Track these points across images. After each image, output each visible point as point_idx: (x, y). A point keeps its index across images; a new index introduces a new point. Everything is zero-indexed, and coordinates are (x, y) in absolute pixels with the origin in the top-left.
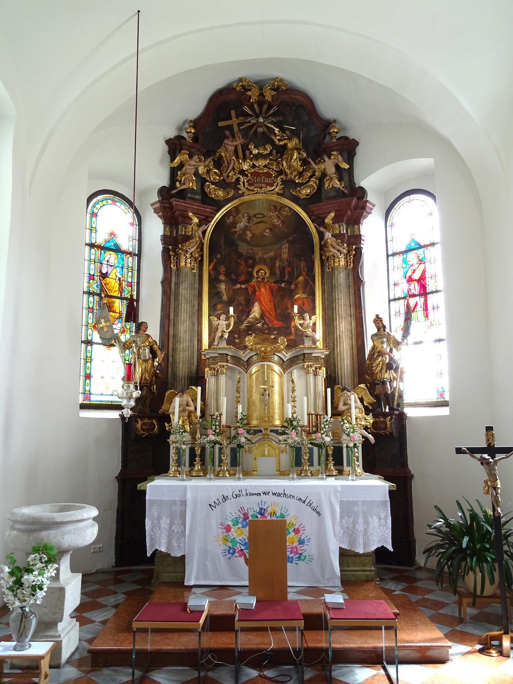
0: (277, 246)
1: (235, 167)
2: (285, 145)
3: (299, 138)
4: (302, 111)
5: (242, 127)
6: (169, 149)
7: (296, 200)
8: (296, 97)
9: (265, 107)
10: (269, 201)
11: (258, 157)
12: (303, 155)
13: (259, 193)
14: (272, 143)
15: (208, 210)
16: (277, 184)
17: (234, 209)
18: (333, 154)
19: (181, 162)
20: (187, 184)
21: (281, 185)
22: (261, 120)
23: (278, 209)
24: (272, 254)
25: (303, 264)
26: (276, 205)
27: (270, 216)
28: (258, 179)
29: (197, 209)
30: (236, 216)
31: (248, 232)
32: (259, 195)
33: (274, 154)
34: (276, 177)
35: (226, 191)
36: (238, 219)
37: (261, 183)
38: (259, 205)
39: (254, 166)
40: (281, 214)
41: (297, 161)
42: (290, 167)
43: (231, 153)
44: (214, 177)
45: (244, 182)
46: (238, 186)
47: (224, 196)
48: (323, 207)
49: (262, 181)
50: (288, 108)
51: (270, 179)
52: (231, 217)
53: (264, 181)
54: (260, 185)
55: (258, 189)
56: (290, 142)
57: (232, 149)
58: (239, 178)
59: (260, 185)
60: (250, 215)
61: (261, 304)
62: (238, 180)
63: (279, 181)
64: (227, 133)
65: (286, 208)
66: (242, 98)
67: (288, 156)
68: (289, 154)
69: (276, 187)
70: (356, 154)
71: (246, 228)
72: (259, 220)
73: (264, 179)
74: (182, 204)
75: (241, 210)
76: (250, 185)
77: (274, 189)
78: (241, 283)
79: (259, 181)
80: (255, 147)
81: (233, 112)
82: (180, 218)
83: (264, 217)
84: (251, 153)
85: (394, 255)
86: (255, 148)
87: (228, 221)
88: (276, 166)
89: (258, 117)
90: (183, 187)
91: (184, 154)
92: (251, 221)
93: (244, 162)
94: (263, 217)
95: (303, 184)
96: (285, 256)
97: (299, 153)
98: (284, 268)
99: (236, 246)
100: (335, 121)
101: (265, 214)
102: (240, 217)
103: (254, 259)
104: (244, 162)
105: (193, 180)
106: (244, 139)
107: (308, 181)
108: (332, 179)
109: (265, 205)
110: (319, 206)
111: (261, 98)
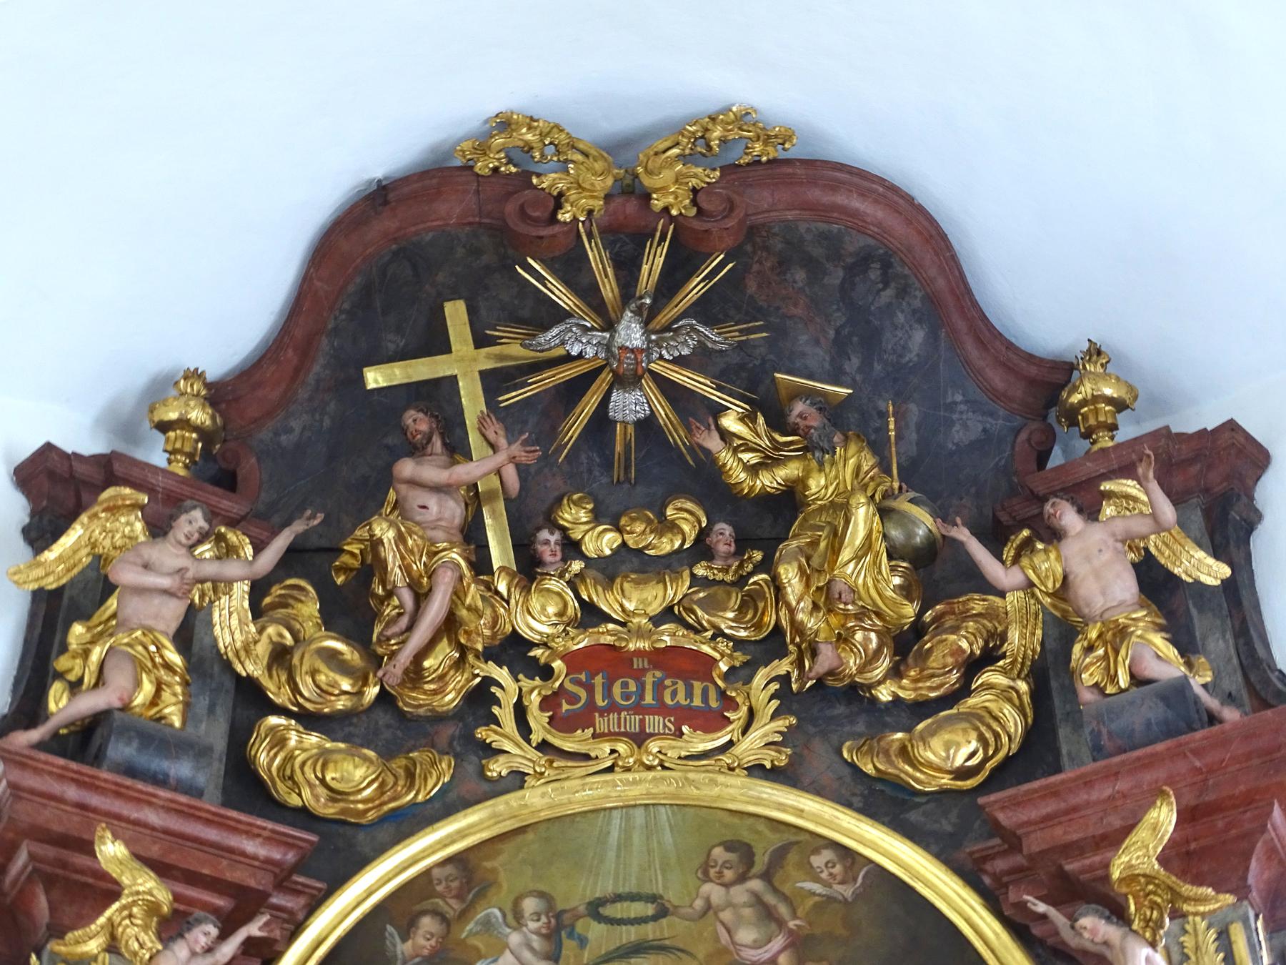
1: (464, 613)
3: (878, 447)
4: (887, 295)
5: (511, 397)
6: (33, 514)
8: (840, 199)
9: (653, 264)
12: (914, 522)
13: (628, 770)
15: (250, 846)
16: (751, 713)
17: (449, 869)
18: (1109, 495)
19: (98, 557)
20: (119, 679)
21: (774, 717)
22: (631, 333)
23: (761, 862)
26: (746, 836)
27: (708, 906)
28: (617, 690)
29: (166, 832)
30: (463, 915)
32: (630, 776)
33: (722, 548)
34: (741, 674)
35: (399, 764)
36: (471, 934)
37: (639, 709)
38: (625, 844)
39: (591, 615)
40: (786, 889)
41: (876, 564)
42: (826, 599)
43: (439, 534)
44: (322, 678)
45: (520, 711)
46: (481, 733)
47: (381, 789)
48: (1083, 797)
49: (649, 699)
50: (800, 275)
51: (698, 686)
52: (427, 923)
53: (658, 695)
54: (632, 722)
55: (622, 748)
56: (821, 464)
57: (447, 514)
58: (488, 681)
59: (632, 722)
60: (560, 906)
63: (764, 696)
64: (417, 422)
65: (816, 851)
66: (511, 208)
67: (814, 544)
68: (821, 528)
69: (745, 731)
70: (1259, 516)
72: (630, 934)
73: (659, 687)
74: (56, 788)
75: (502, 877)
76: (560, 723)
77: (730, 744)
79: (626, 696)
80: (597, 517)
81: (456, 314)
82: (42, 904)
83: (662, 913)
86: (597, 517)
87: (404, 948)
88: (741, 610)
89: (610, 325)
90: (89, 703)
91: (113, 510)
92: (569, 946)
93: (526, 590)
94: (655, 918)
95: (922, 709)
97: (884, 513)
100: (1099, 353)
101: (672, 896)
102: (487, 924)
104: (526, 590)
105: (168, 666)
106: (525, 443)
107: (963, 691)
108: (1122, 633)
109: (668, 838)
110: (1054, 793)
111: (632, 207)
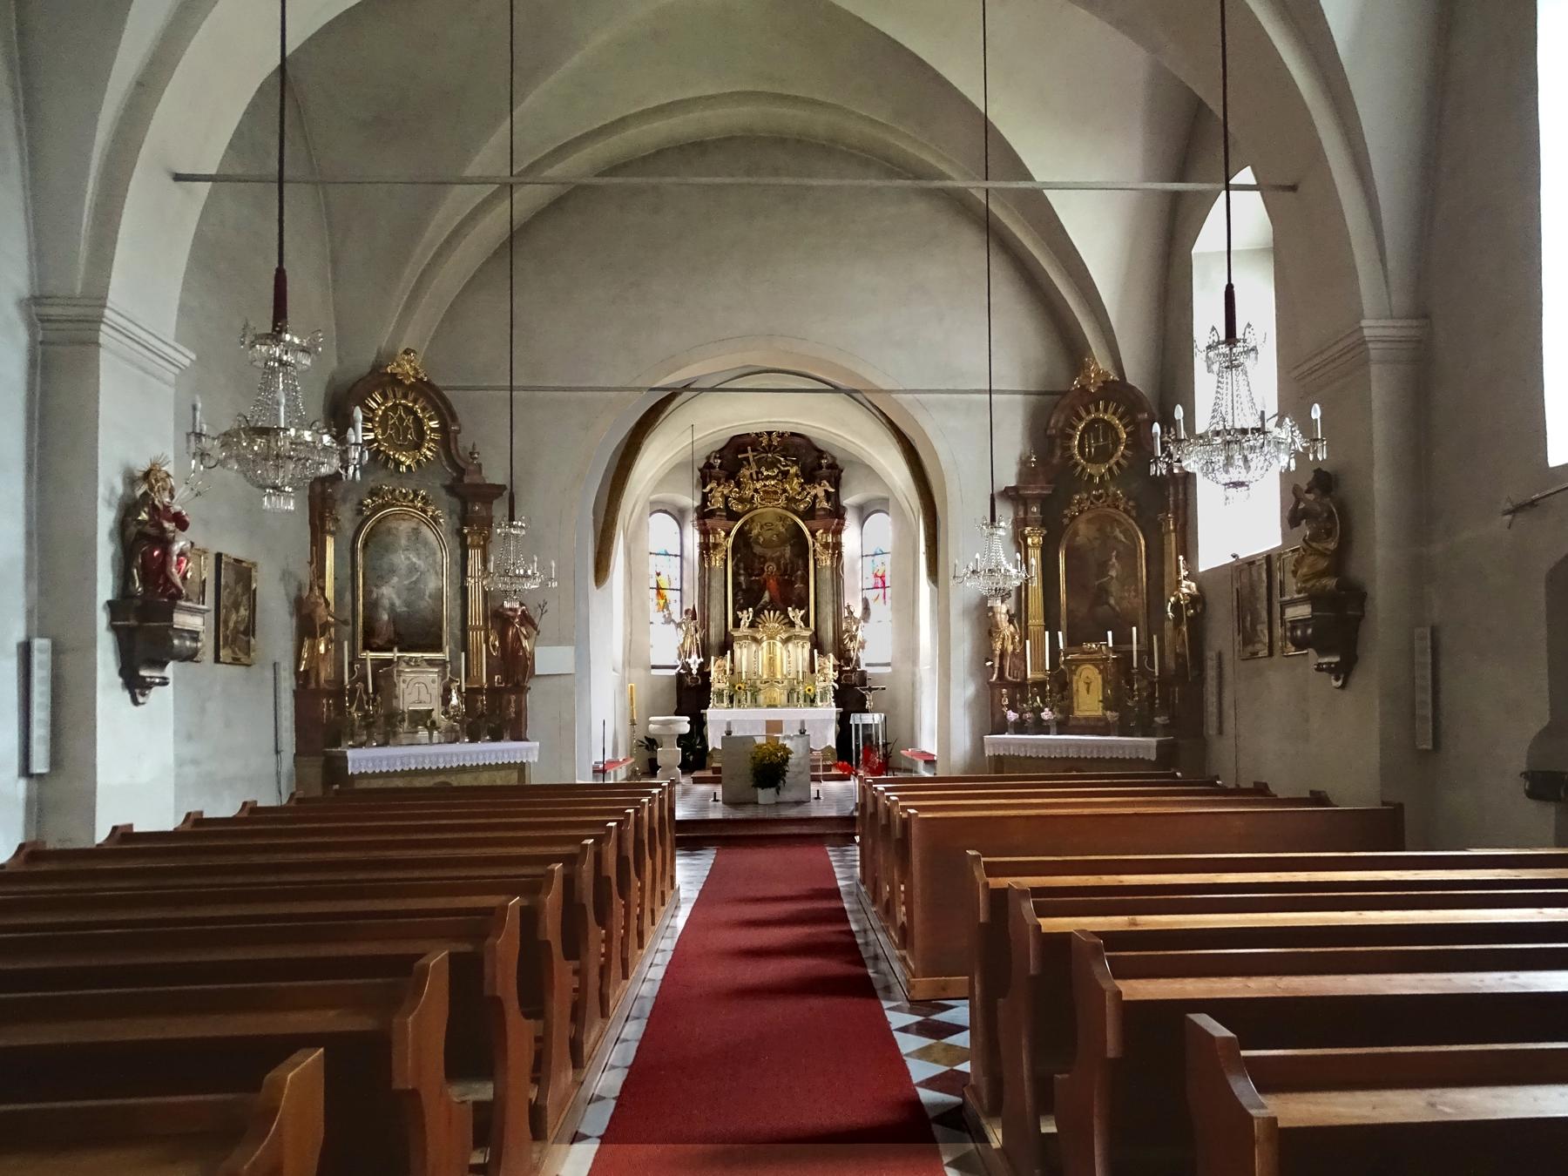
0: (783, 548)
2: (789, 470)
7: (796, 512)
10: (776, 513)
11: (768, 478)
14: (779, 468)
24: (778, 554)
25: (800, 563)
31: (760, 537)
39: (765, 486)
61: (770, 592)
62: (753, 496)
64: (745, 463)
71: (759, 534)
76: (762, 500)
78: (756, 576)
81: (749, 448)
84: (763, 474)
85: (866, 556)
96: (787, 556)
98: (787, 564)
99: (752, 548)
103: (765, 558)
